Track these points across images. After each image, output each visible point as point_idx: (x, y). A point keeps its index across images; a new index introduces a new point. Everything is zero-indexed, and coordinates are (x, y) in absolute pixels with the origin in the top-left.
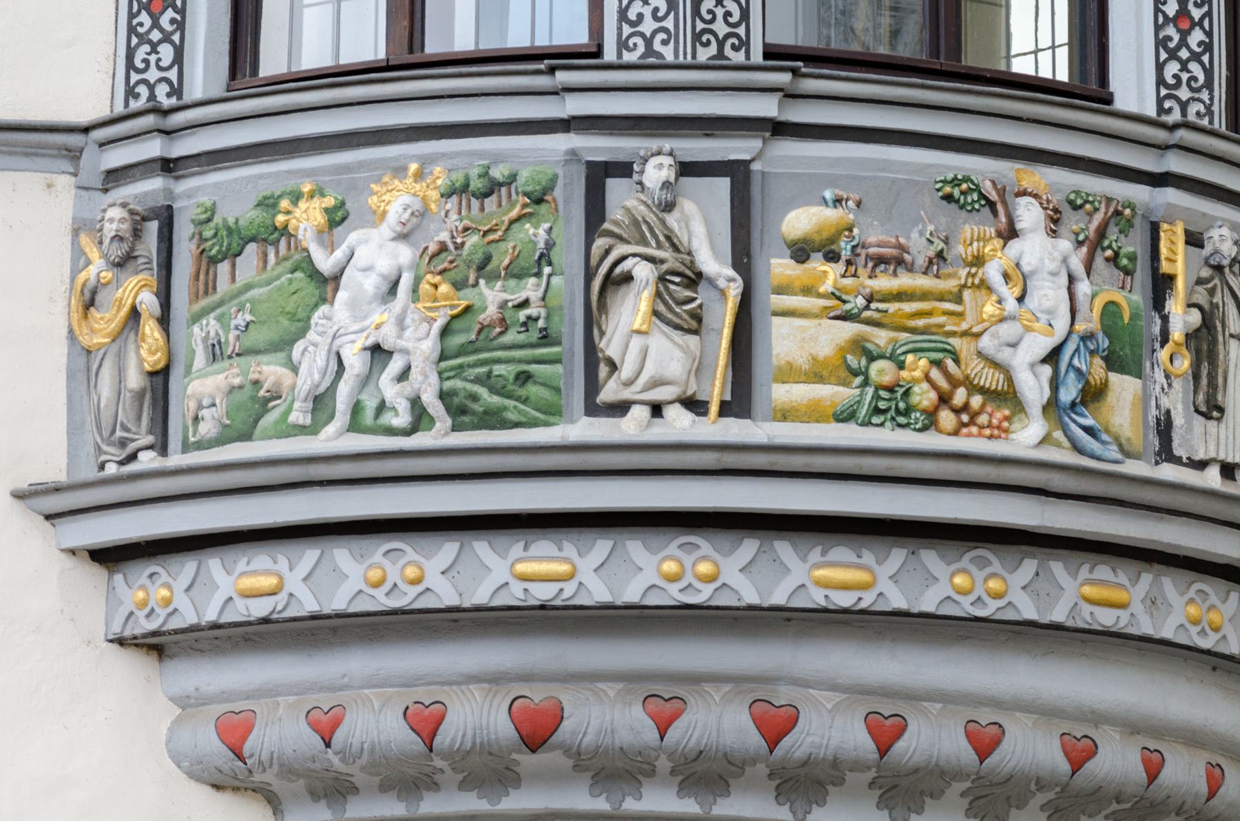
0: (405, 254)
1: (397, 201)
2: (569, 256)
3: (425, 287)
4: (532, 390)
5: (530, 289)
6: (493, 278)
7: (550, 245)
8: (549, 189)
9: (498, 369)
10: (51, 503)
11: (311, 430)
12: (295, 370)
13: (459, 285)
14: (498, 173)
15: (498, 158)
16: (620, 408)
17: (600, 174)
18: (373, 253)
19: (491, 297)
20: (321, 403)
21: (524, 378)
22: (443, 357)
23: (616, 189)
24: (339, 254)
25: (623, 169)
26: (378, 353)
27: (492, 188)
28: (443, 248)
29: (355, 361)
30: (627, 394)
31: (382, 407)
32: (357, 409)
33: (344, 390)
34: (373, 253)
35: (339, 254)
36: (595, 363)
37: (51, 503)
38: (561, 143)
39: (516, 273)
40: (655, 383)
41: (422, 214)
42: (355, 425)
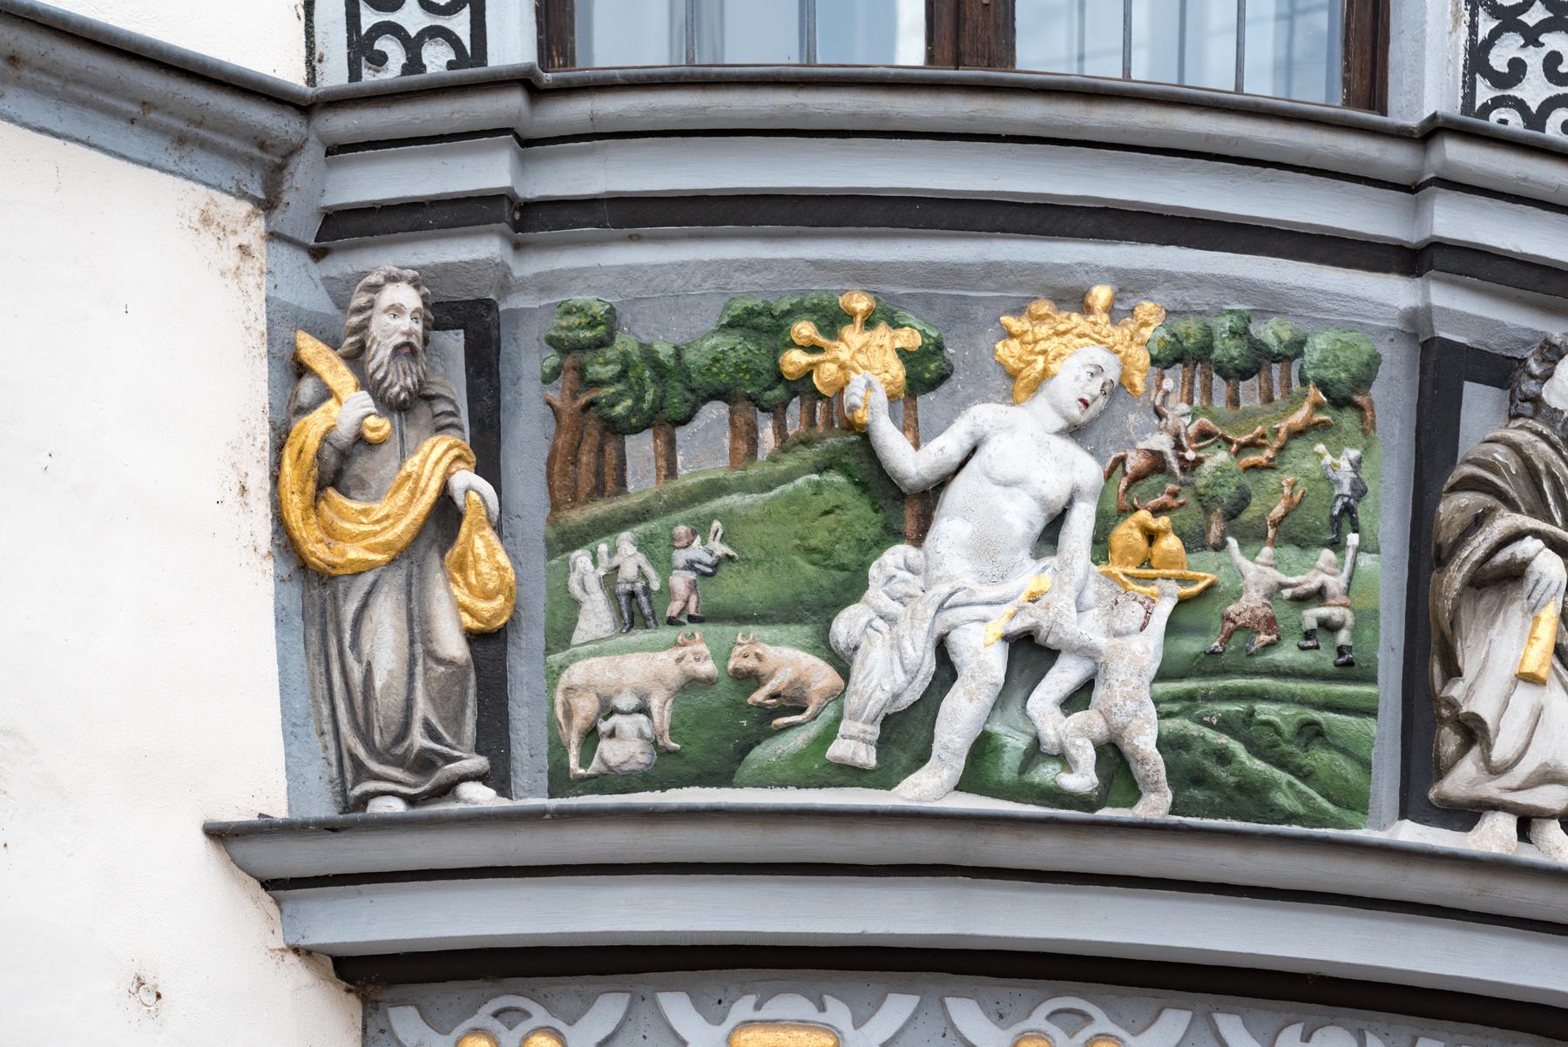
0: (1086, 470)
1: (1082, 359)
2: (1387, 517)
3: (1127, 533)
4: (1320, 758)
5: (1320, 568)
6: (1252, 537)
7: (1359, 491)
8: (1363, 381)
9: (1266, 711)
10: (271, 860)
11: (883, 777)
12: (842, 664)
13: (1194, 541)
14: (1270, 332)
15: (1272, 302)
16: (1466, 814)
17: (1444, 369)
18: (1015, 457)
19: (1255, 573)
20: (905, 735)
21: (1312, 733)
22: (1161, 676)
23: (1480, 408)
24: (946, 446)
25: (1499, 369)
26: (1030, 652)
27: (1257, 361)
28: (1157, 463)
29: (983, 658)
30: (1492, 789)
31: (1036, 752)
32: (983, 748)
33: (960, 718)
34: (1015, 457)
35: (946, 446)
36: (1434, 726)
37: (271, 860)
38: (1394, 293)
39: (1296, 535)
40: (1548, 776)
41: (1118, 391)
42: (966, 784)
